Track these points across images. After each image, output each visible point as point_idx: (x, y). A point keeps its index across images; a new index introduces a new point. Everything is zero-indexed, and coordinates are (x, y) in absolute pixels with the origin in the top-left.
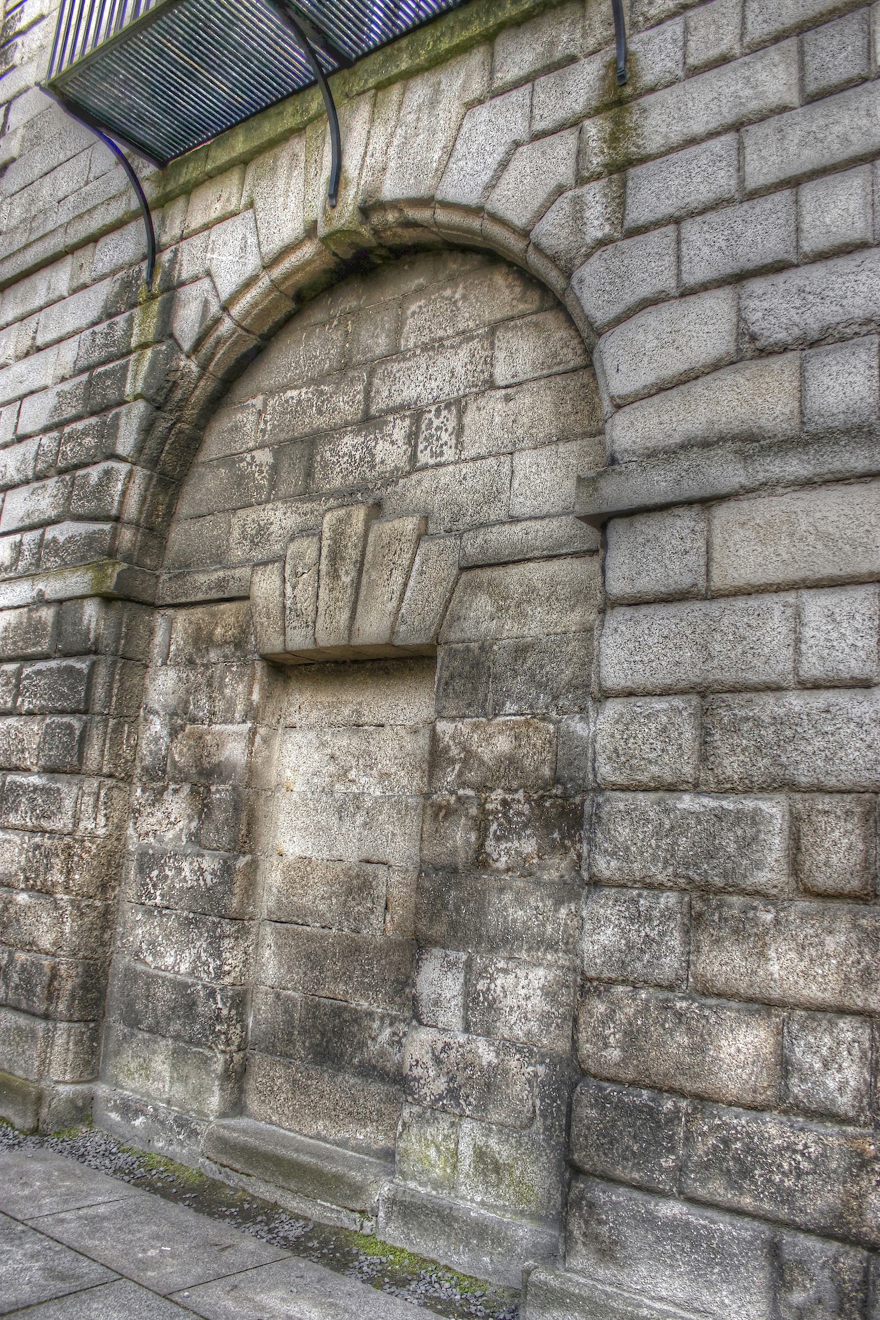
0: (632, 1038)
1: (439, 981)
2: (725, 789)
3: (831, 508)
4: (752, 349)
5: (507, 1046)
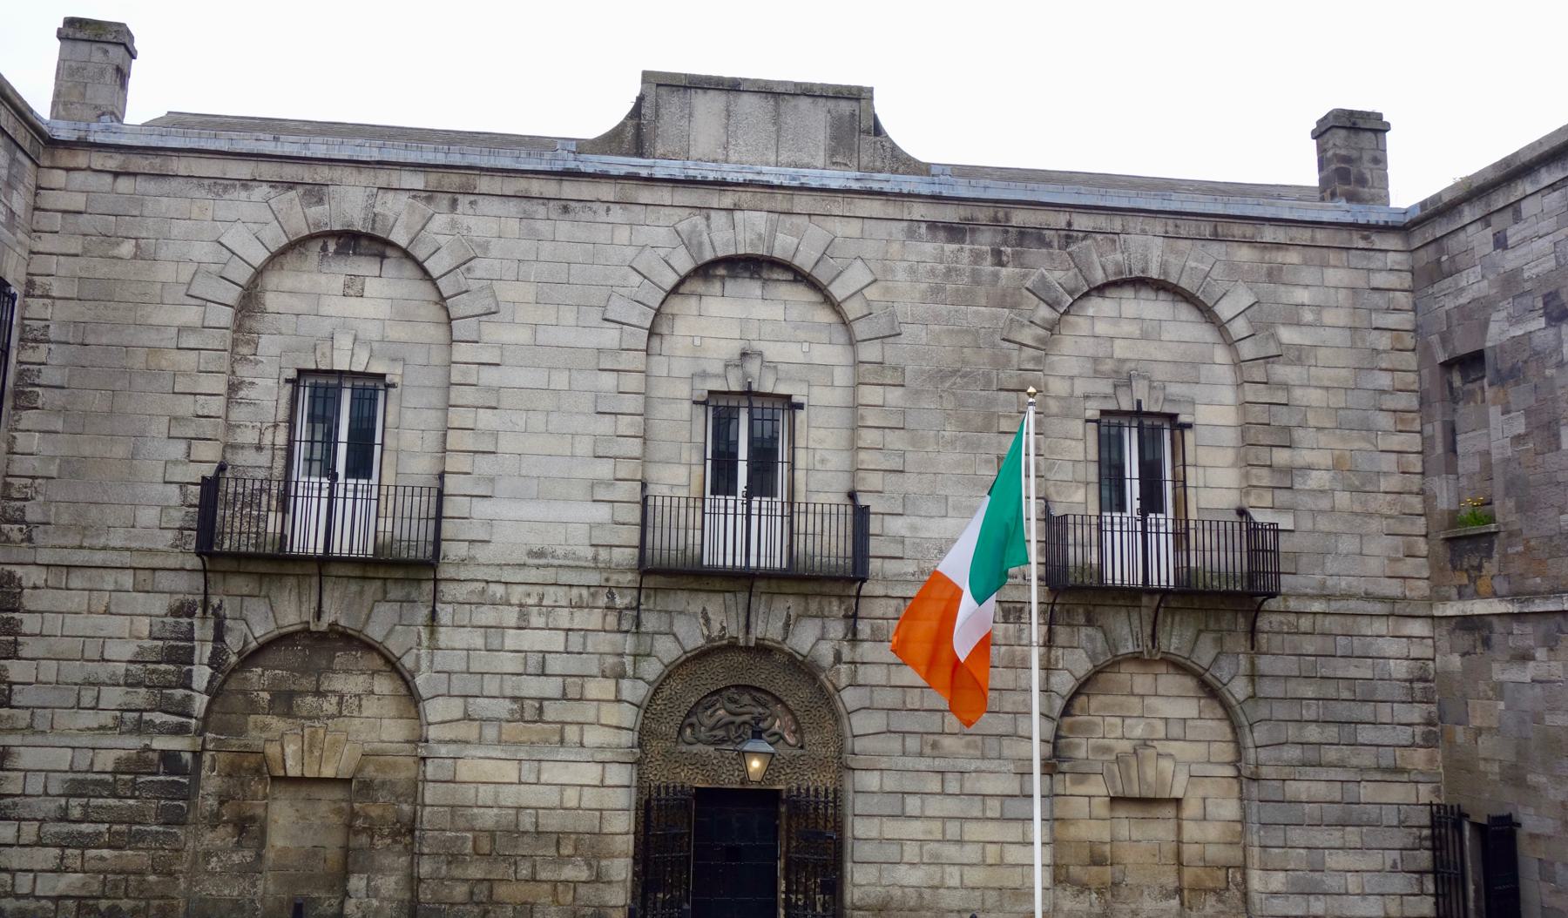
0: (434, 893)
1: (357, 883)
2: (457, 831)
3: (488, 764)
4: (467, 717)
5: (383, 899)
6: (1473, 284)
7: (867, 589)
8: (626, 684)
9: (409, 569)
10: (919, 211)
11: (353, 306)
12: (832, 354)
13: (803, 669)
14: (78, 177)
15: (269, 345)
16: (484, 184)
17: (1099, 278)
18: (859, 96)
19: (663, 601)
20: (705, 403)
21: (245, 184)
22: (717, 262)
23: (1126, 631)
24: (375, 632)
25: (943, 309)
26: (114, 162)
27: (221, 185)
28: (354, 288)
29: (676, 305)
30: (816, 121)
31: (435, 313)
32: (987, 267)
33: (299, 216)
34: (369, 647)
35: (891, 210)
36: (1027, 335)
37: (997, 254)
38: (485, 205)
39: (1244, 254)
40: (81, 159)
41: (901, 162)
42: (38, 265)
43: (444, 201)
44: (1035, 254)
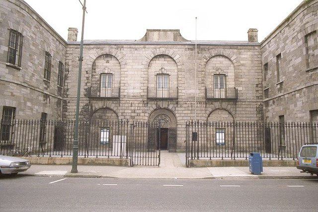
6: (266, 53)
7: (179, 100)
8: (146, 114)
9: (116, 99)
10: (186, 47)
11: (108, 64)
12: (174, 68)
13: (171, 111)
14: (71, 49)
15: (97, 70)
16: (125, 46)
17: (213, 55)
18: (178, 31)
19: (151, 102)
20: (156, 75)
21: (93, 48)
22: (158, 55)
23: (217, 105)
24: (112, 108)
25: (190, 61)
26: (76, 47)
27: (90, 49)
28: (108, 62)
29: (152, 62)
30: (171, 35)
31: (118, 65)
32: (197, 54)
33: (100, 52)
34: (111, 110)
35: (183, 47)
36: (203, 64)
37: (198, 52)
38: (126, 49)
39: (235, 50)
40: (72, 46)
41: (184, 40)
42: (67, 61)
43: (119, 49)
44: (204, 52)
